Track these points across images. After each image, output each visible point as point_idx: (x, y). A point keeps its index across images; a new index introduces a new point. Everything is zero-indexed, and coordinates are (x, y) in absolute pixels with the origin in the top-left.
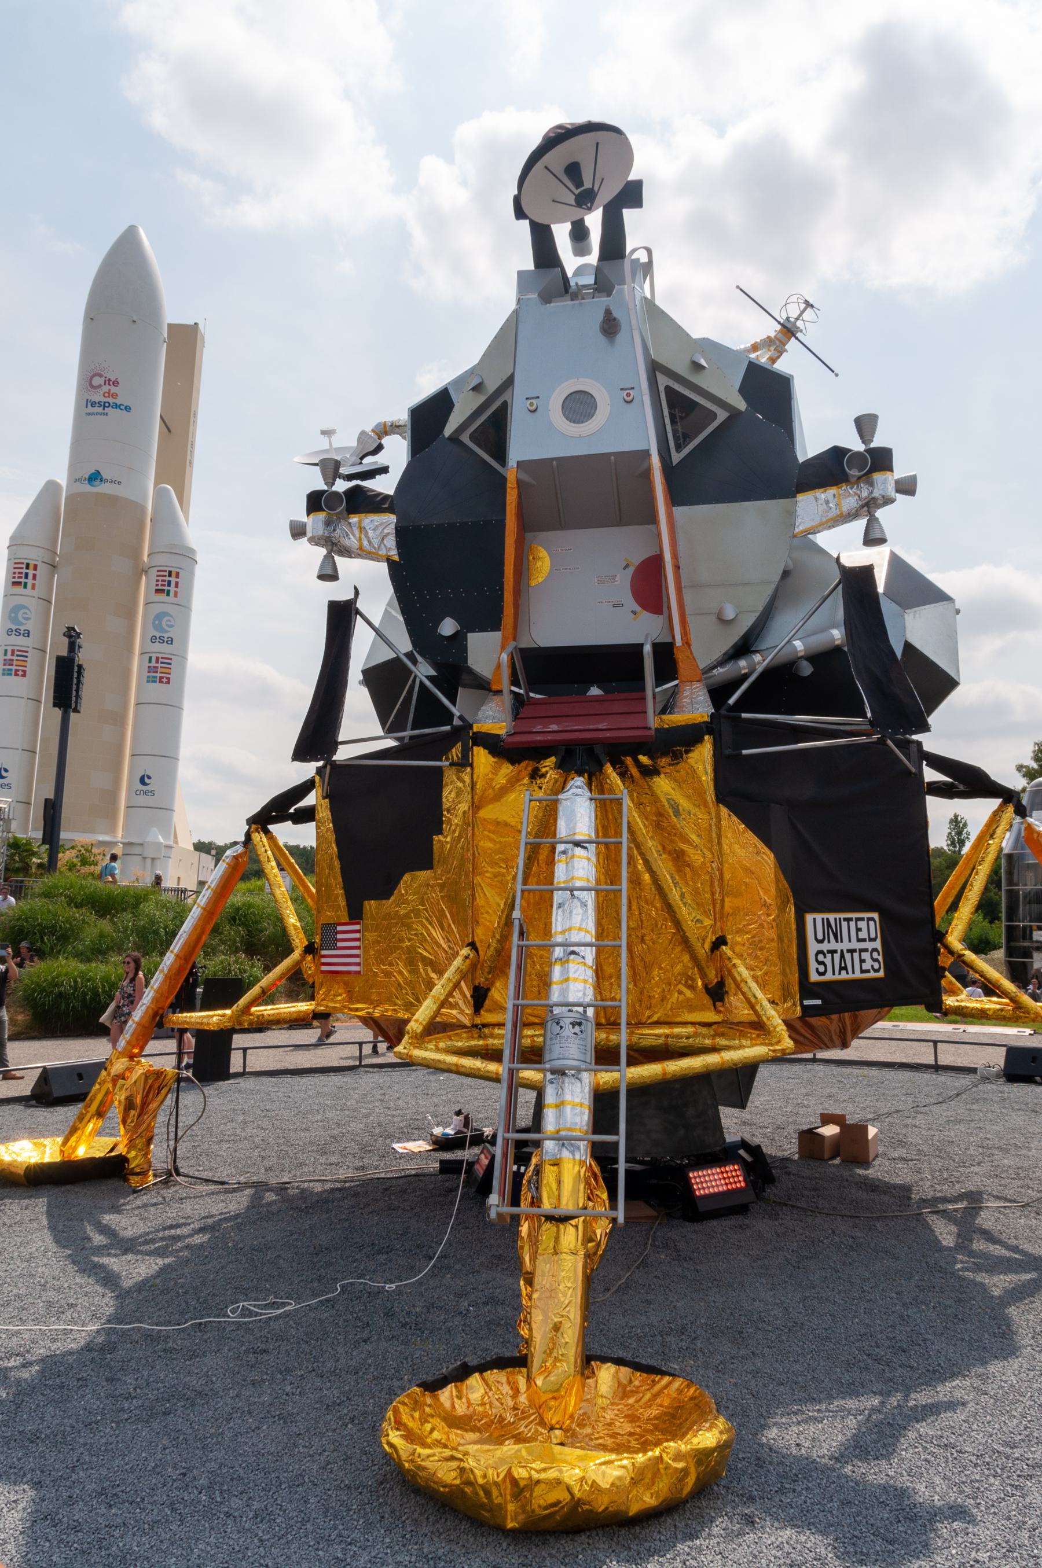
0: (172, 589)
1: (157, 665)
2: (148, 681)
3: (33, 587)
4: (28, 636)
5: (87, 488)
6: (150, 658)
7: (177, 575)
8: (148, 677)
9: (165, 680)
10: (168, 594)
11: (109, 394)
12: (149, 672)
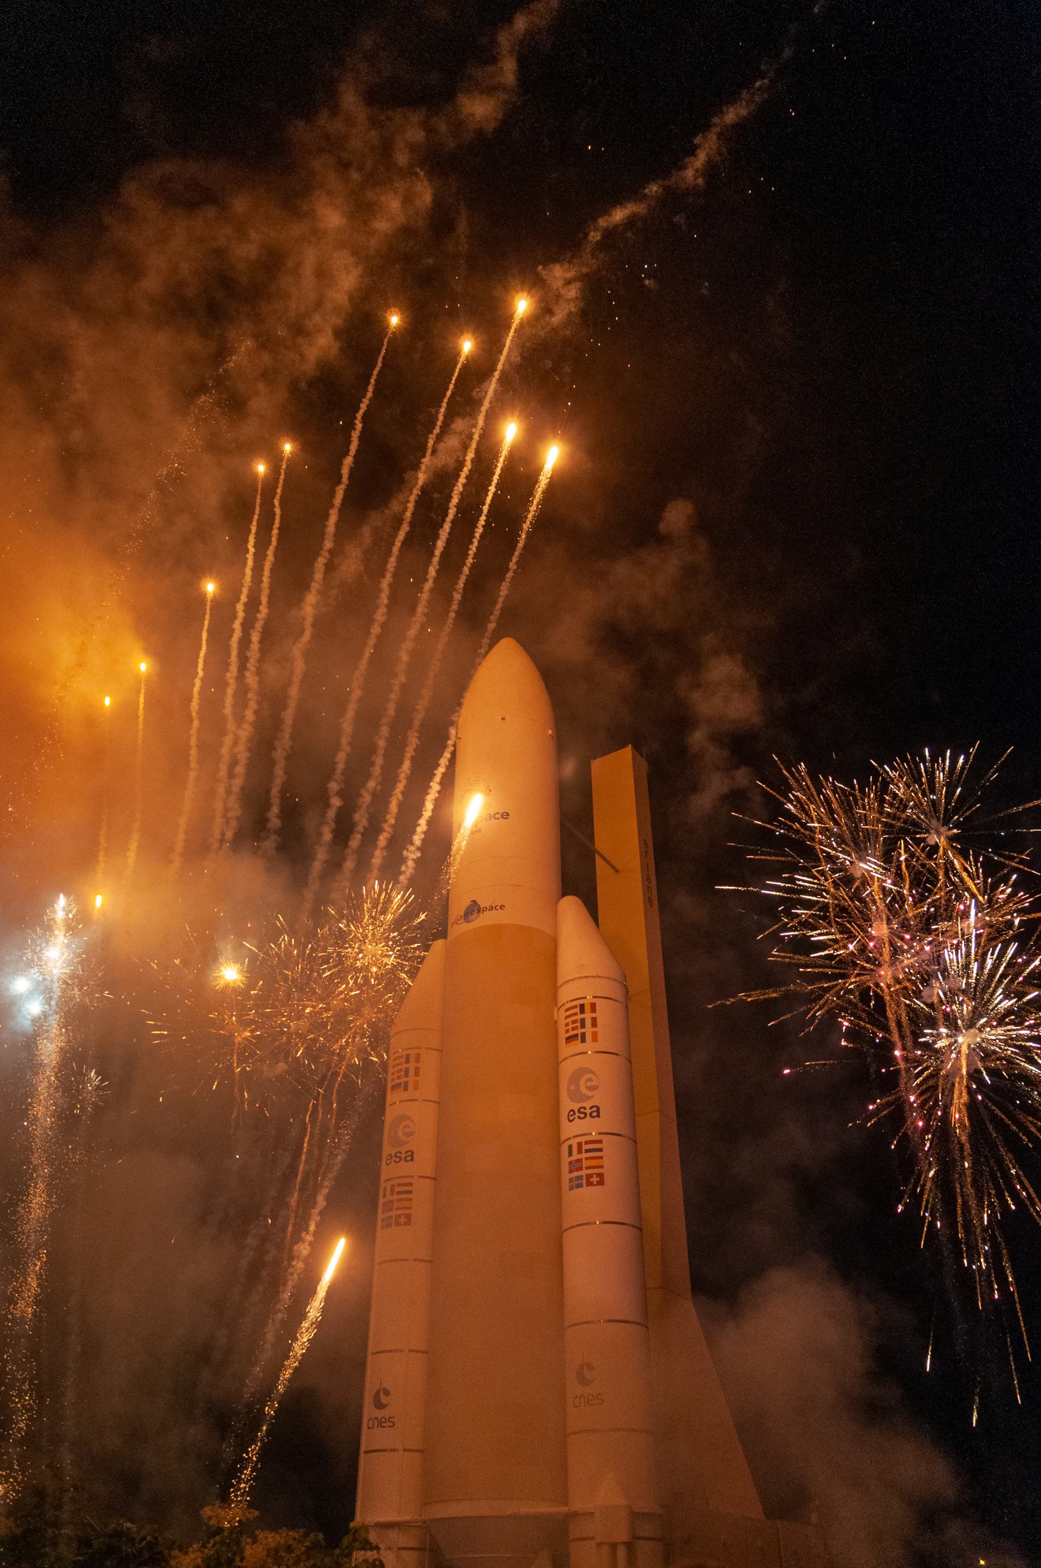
0: (588, 1030)
1: (579, 1156)
2: (571, 1188)
3: (416, 1088)
4: (412, 1160)
6: (570, 1147)
7: (593, 1008)
8: (571, 1180)
9: (595, 1180)
10: (583, 1040)
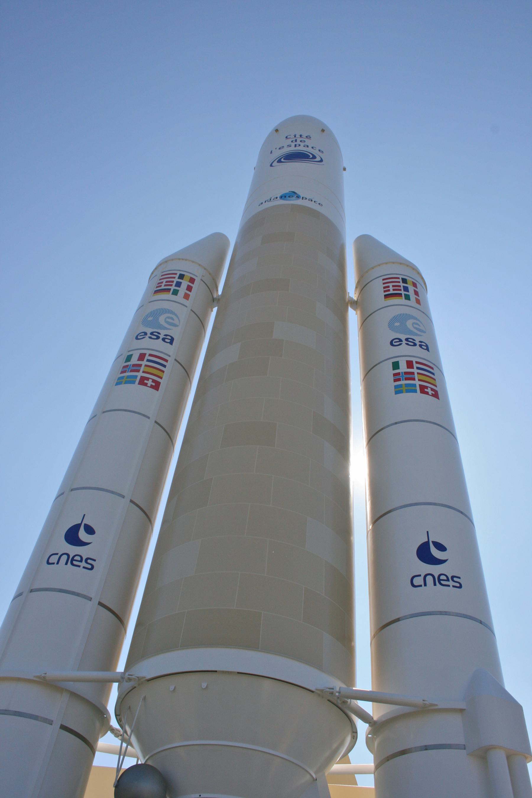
9: (150, 383)
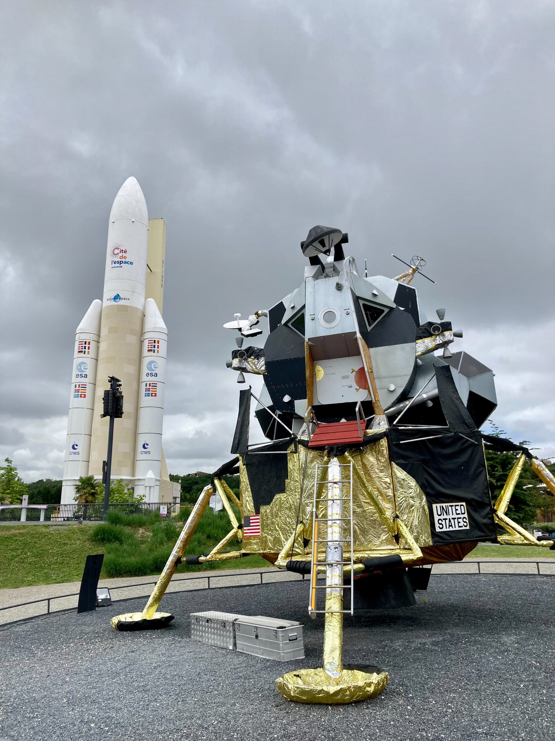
1: (150, 387)
5: (113, 303)
6: (146, 384)
8: (146, 394)
9: (154, 395)
11: (122, 257)
12: (146, 391)
